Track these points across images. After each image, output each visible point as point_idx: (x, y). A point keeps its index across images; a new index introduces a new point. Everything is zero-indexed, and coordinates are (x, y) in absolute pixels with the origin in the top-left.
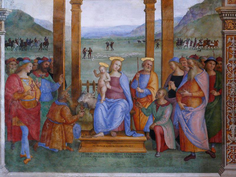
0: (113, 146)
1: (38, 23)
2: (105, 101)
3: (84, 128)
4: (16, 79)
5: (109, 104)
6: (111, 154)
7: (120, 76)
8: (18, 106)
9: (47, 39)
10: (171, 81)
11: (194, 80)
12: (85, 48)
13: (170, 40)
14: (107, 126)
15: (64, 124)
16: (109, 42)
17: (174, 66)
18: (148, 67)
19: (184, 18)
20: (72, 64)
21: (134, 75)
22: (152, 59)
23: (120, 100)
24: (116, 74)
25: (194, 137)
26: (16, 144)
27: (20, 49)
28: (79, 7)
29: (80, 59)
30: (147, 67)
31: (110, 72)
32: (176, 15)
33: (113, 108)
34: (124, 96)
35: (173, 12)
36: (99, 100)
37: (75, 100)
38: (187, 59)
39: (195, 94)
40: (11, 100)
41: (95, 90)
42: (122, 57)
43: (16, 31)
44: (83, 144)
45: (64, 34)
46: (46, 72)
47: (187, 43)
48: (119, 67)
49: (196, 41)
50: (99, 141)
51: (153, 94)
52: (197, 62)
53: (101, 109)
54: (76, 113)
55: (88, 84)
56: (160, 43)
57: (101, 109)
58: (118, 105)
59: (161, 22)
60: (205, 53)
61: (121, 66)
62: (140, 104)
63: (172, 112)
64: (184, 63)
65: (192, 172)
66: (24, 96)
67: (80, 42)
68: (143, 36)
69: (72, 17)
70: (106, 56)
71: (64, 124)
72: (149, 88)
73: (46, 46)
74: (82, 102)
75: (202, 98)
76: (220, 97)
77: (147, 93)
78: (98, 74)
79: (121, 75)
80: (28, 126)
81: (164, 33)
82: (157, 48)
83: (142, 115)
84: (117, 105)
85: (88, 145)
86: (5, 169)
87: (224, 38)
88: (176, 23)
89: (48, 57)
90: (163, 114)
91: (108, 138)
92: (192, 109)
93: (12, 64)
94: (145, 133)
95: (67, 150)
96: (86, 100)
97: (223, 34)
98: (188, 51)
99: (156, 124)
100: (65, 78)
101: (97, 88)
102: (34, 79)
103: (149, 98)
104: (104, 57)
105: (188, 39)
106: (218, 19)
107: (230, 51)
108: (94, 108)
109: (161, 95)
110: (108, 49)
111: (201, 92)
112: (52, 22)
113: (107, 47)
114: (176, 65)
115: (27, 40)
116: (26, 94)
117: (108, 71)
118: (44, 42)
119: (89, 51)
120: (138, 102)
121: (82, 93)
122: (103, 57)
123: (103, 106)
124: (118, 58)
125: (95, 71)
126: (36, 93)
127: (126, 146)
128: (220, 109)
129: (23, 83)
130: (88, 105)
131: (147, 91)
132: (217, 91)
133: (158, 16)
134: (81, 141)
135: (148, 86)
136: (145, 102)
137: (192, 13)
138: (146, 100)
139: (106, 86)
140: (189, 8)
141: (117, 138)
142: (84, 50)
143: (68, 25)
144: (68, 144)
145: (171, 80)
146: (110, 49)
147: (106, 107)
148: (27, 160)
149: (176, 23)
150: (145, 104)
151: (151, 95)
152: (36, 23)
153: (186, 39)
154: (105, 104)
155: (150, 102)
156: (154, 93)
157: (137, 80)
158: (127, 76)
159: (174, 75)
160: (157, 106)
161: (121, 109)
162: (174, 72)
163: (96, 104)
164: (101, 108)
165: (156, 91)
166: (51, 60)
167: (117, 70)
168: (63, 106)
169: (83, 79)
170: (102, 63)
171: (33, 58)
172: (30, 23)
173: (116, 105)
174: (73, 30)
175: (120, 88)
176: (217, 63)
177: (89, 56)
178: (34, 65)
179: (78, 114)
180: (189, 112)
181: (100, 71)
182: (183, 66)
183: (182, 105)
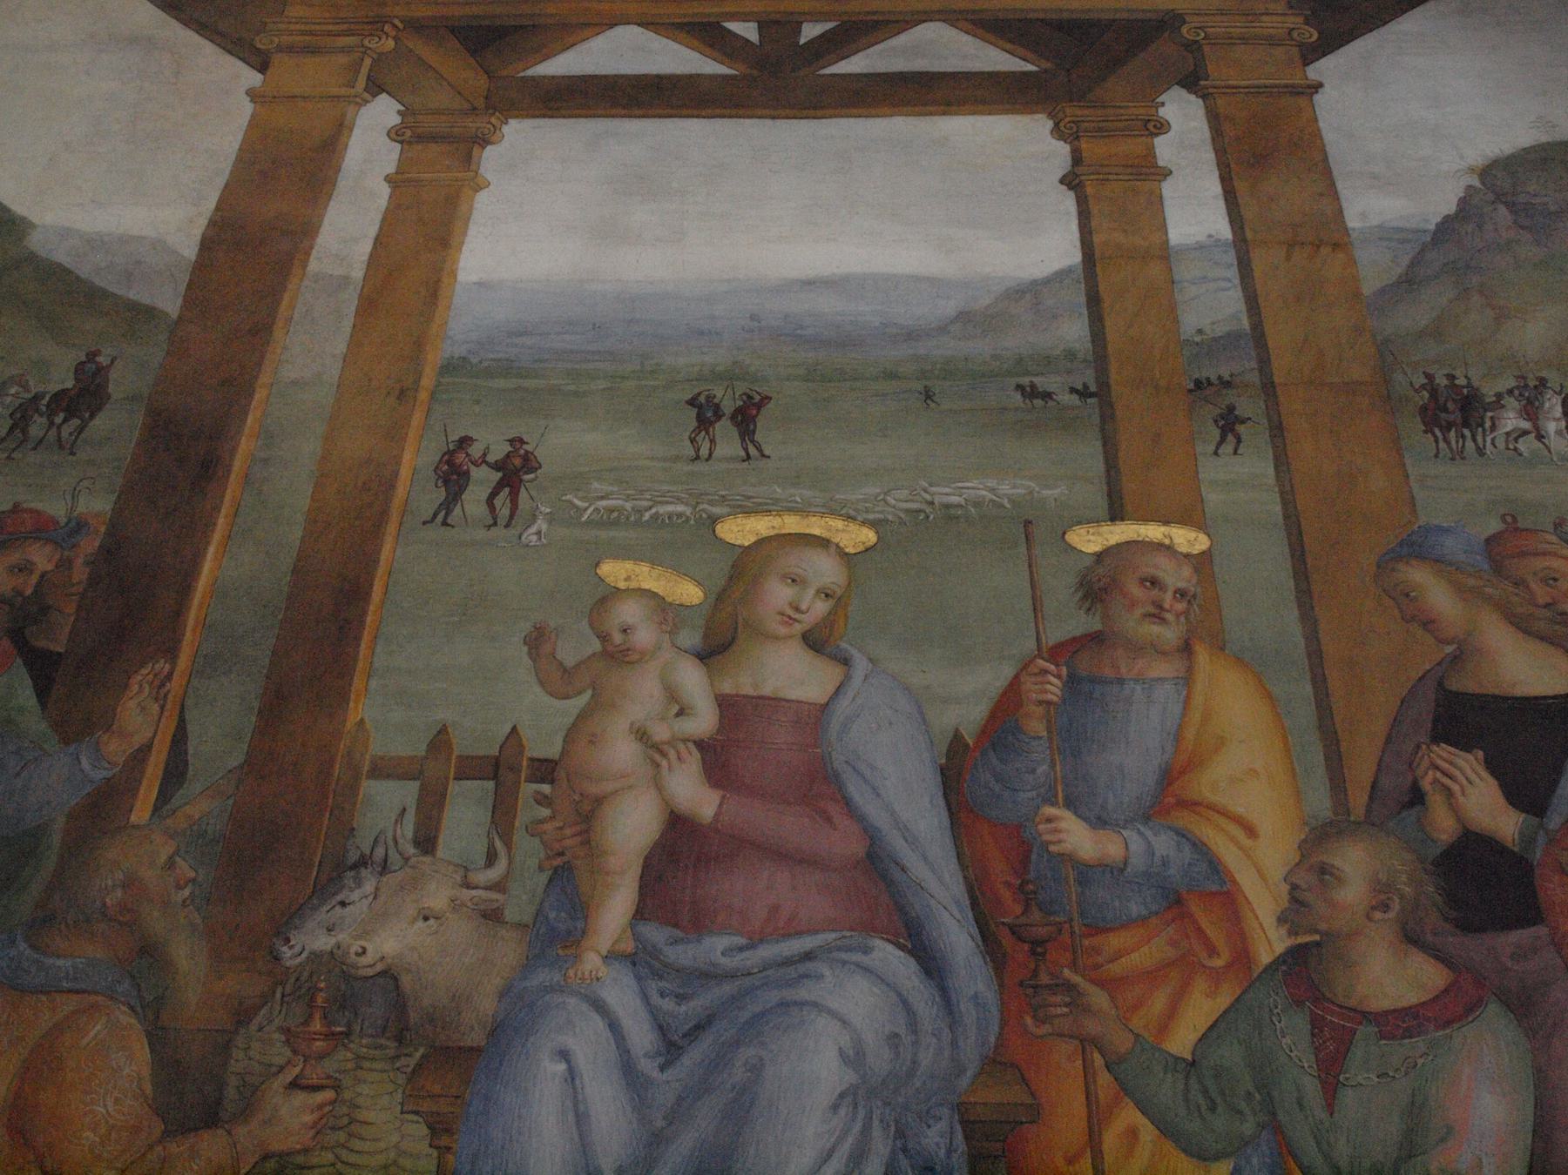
2: (632, 960)
5: (681, 998)
7: (831, 689)
9: (100, 370)
10: (1443, 751)
12: (465, 442)
16: (719, 392)
17: (1439, 597)
18: (1152, 610)
19: (1447, 228)
20: (295, 571)
21: (989, 679)
22: (1187, 539)
23: (828, 949)
28: (468, 161)
29: (391, 528)
30: (1139, 611)
32: (1363, 215)
33: (736, 1043)
35: (1332, 191)
41: (520, 838)
42: (849, 518)
45: (278, 333)
47: (1531, 411)
48: (821, 608)
51: (1247, 881)
53: (564, 1055)
54: (219, 1102)
56: (1249, 406)
57: (564, 1055)
58: (801, 1004)
59: (1231, 257)
61: (839, 592)
62: (1099, 998)
63: (1538, 1104)
67: (423, 396)
68: (1070, 355)
69: (384, 219)
70: (680, 508)
72: (1183, 819)
73: (76, 422)
74: (333, 960)
77: (1172, 871)
78: (578, 666)
79: (847, 678)
81: (1280, 337)
82: (1228, 448)
83: (1132, 1133)
84: (784, 1005)
89: (57, 509)
100: (189, 702)
101: (545, 812)
103: (1199, 930)
104: (656, 517)
105: (1532, 383)
108: (476, 1038)
109: (1353, 892)
110: (704, 452)
113: (698, 430)
117: (691, 638)
118: (69, 384)
119: (497, 466)
120: (1067, 972)
121: (353, 857)
122: (647, 516)
123: (599, 1023)
124: (816, 527)
125: (537, 641)
130: (400, 1004)
131: (1164, 844)
136: (1153, 976)
137: (1506, 204)
138: (1171, 953)
139: (659, 788)
140: (1472, 170)
142: (449, 457)
143: (339, 272)
145: (1436, 739)
146: (727, 442)
147: (641, 1037)
150: (1159, 1002)
151: (1228, 899)
152: (42, 253)
153: (1512, 383)
154: (621, 993)
155: (1216, 977)
157: (1037, 727)
158: (907, 689)
160: (1317, 1024)
161: (841, 1053)
162: (1457, 659)
163: (503, 994)
164: (571, 1043)
166: (79, 526)
167: (798, 629)
168: (69, 1004)
170: (629, 565)
173: (763, 1014)
174: (369, 305)
175: (834, 810)
177: (498, 502)
179: (248, 1107)
181: (604, 638)
182: (1541, 601)
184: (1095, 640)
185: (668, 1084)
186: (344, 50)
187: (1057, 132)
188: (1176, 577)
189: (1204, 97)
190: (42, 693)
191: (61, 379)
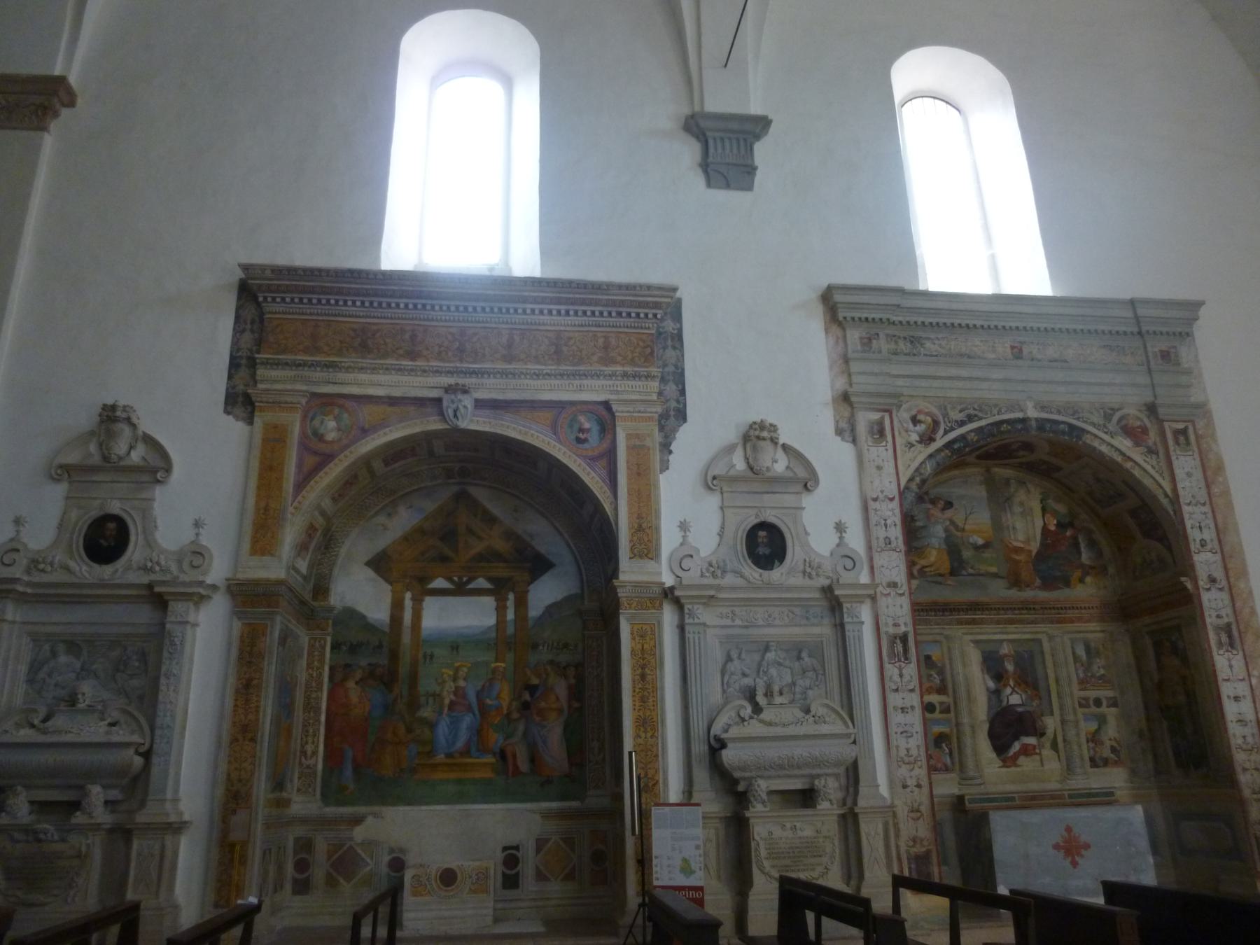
17: (529, 672)
22: (503, 665)
24: (462, 683)
31: (455, 679)
34: (469, 709)
36: (440, 713)
47: (543, 646)
49: (553, 644)
60: (563, 658)
75: (560, 711)
88: (531, 623)
94: (494, 754)
99: (507, 743)
125: (436, 680)
133: (510, 615)
135: (498, 697)
146: (455, 652)
147: (449, 723)
149: (531, 623)
156: (505, 704)
171: (364, 662)
183: (537, 719)
187: (495, 600)
188: (501, 670)
189: (514, 593)
191: (377, 643)
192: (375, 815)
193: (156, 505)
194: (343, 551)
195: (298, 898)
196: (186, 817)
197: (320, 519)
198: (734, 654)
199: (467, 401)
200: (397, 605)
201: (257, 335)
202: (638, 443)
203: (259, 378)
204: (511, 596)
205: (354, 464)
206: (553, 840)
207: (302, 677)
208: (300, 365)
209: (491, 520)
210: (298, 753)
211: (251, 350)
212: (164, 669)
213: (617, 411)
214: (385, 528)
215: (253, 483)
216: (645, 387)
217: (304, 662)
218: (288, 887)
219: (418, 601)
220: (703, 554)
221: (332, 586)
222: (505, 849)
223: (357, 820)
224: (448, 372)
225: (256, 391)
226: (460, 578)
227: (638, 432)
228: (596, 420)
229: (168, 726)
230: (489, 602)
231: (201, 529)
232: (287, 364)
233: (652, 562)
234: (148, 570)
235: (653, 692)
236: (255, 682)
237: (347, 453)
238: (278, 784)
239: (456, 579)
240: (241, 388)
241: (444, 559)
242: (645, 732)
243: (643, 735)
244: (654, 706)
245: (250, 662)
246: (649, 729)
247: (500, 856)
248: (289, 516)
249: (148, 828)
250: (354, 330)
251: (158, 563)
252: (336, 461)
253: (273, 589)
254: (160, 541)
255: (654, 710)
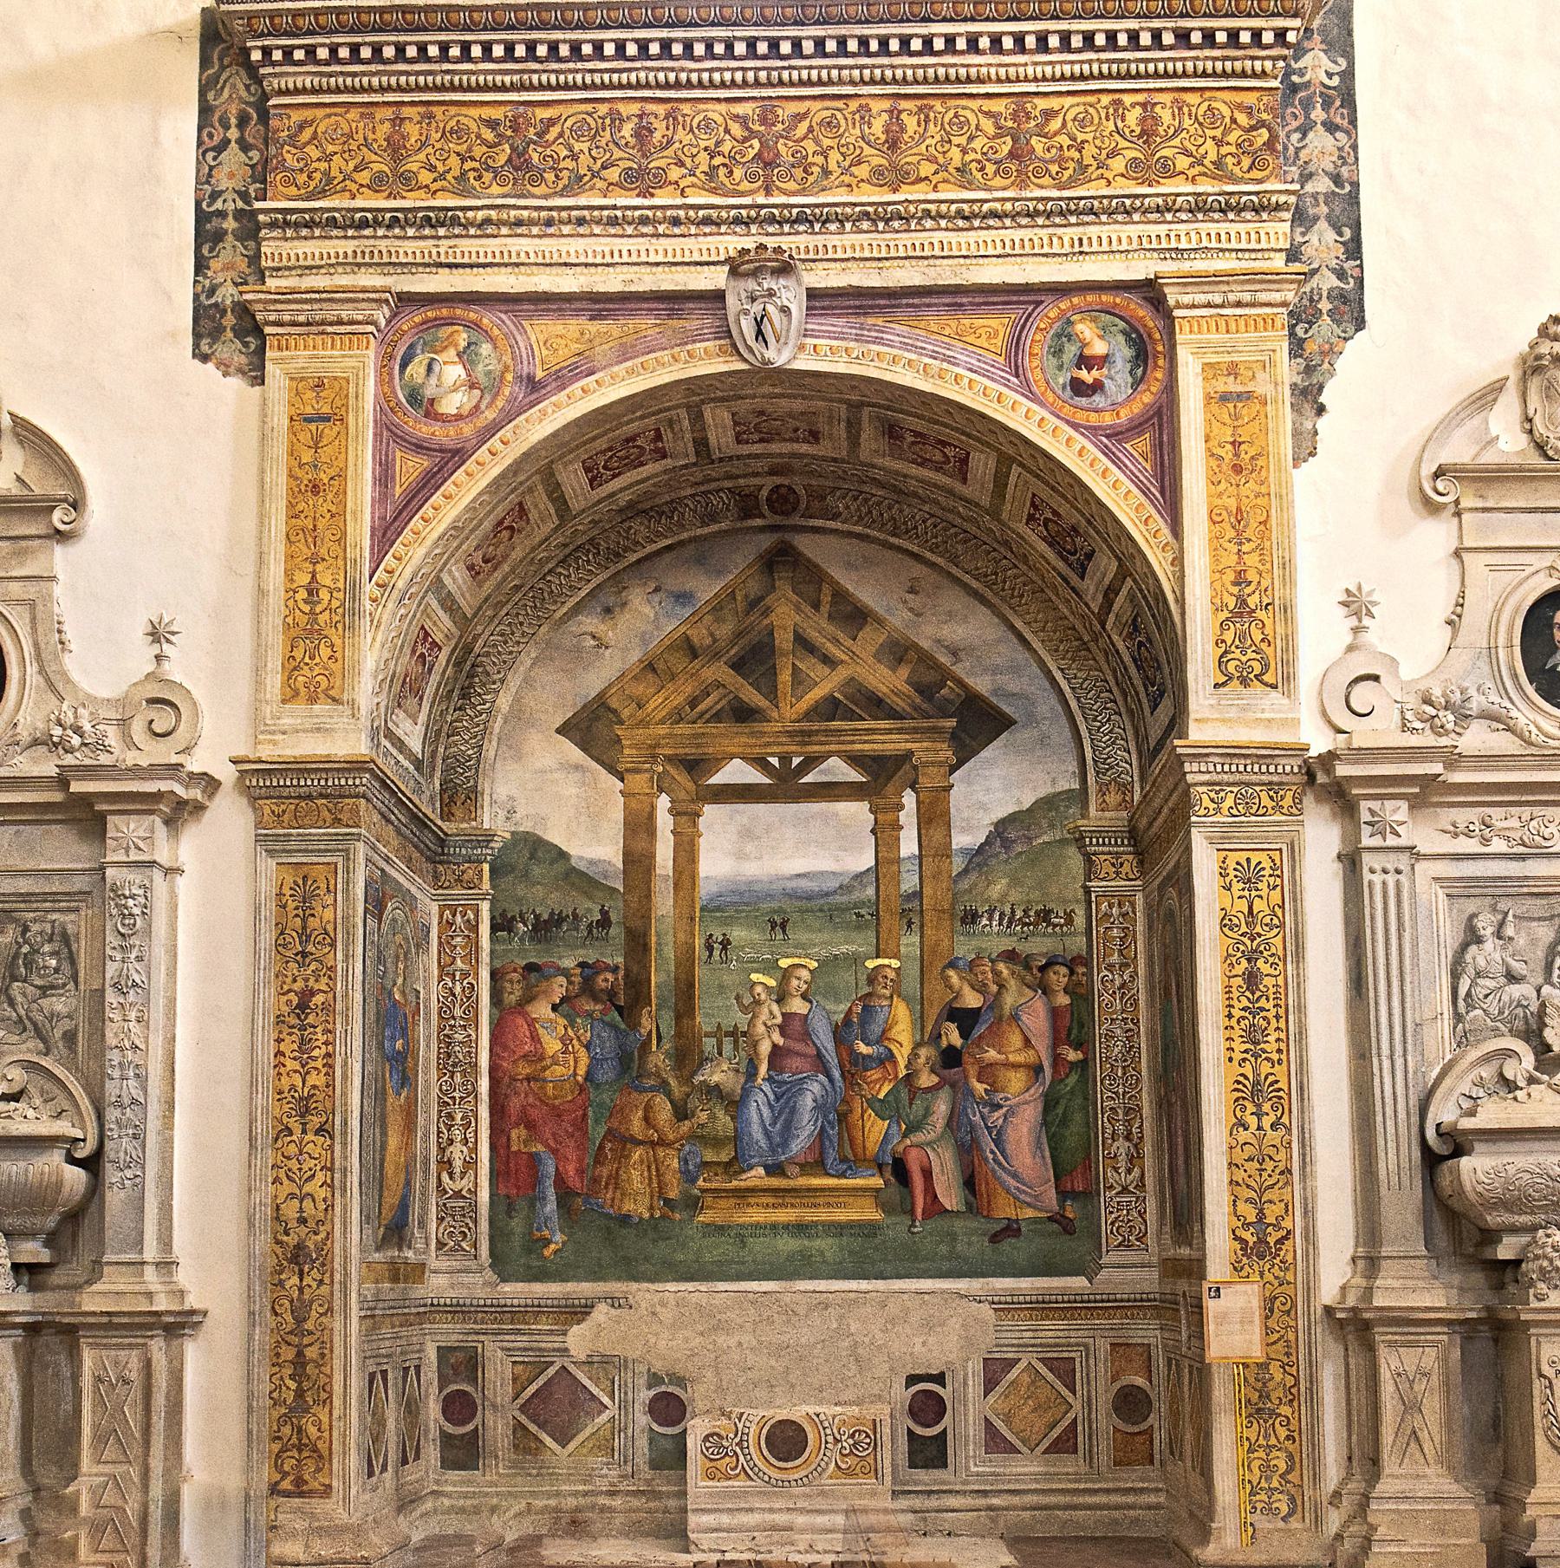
0: (793, 1206)
1: (582, 866)
3: (709, 1156)
4: (520, 1021)
6: (786, 1226)
8: (526, 1095)
11: (1015, 1018)
13: (943, 911)
14: (773, 1150)
15: (653, 1145)
21: (844, 1007)
22: (895, 963)
24: (798, 1006)
25: (1015, 1176)
26: (521, 1204)
27: (532, 939)
28: (695, 824)
37: (688, 1080)
38: (992, 961)
39: (1012, 1058)
40: (506, 1079)
43: (521, 891)
44: (709, 1200)
46: (603, 1003)
47: (990, 919)
49: (1013, 912)
50: (752, 1191)
51: (899, 1058)
52: (1017, 968)
55: (719, 1033)
56: (916, 920)
60: (1039, 946)
64: (984, 973)
65: (1014, 1276)
66: (545, 1069)
71: (653, 1144)
72: (886, 1043)
75: (1037, 1070)
76: (1084, 1065)
80: (555, 1152)
81: (927, 891)
85: (723, 1203)
86: (489, 1275)
87: (1089, 903)
88: (958, 864)
89: (609, 961)
90: (928, 1112)
91: (775, 1182)
92: (1007, 1099)
93: (511, 982)
94: (880, 1167)
95: (663, 1217)
96: (716, 1078)
97: (1087, 891)
98: (993, 938)
99: (908, 1142)
102: (572, 1024)
106: (1072, 851)
107: (1107, 939)
109: (922, 1060)
111: (1031, 1052)
112: (621, 866)
114: (961, 978)
115: (552, 914)
116: (549, 1062)
117: (774, 997)
125: (738, 998)
126: (576, 1062)
127: (829, 1205)
128: (1086, 1099)
129: (541, 1031)
132: (1076, 1050)
133: (909, 845)
134: (704, 1191)
135: (883, 1037)
141: (803, 1181)
144: (667, 1201)
147: (772, 1097)
148: (553, 1246)
151: (895, 1063)
154: (766, 1087)
159: (956, 1005)
165: (906, 1050)
166: (615, 969)
169: (703, 1022)
172: (559, 867)
174: (676, 885)
176: (1072, 972)
178: (570, 982)
180: (1000, 1107)
183: (980, 1088)
184: (869, 995)
185: (777, 1106)
186: (646, 771)
188: (891, 975)
190: (621, 1015)
192: (614, 1301)
193: (58, 590)
194: (504, 702)
195: (454, 1475)
196: (192, 1302)
197: (446, 620)
198: (1485, 925)
199: (791, 294)
200: (639, 827)
201: (255, 155)
202: (1233, 387)
203: (270, 264)
204: (909, 799)
205: (515, 468)
206: (1022, 1365)
207: (431, 992)
208: (364, 224)
209: (854, 616)
210: (433, 1167)
211: (244, 196)
212: (111, 969)
213: (1178, 306)
214: (602, 644)
215: (278, 522)
216: (1253, 236)
217: (430, 961)
218: (432, 1453)
219: (686, 815)
220: (1406, 673)
221: (485, 785)
222: (912, 1380)
223: (578, 1312)
224: (737, 221)
225: (262, 296)
226: (785, 759)
227: (1236, 358)
228: (1123, 332)
229: (134, 1102)
230: (858, 812)
231: (165, 646)
232: (332, 223)
233: (1274, 694)
234: (55, 745)
235: (1277, 1017)
236: (319, 999)
237: (494, 442)
238: (395, 1231)
239: (774, 761)
240: (227, 294)
241: (743, 714)
242: (1259, 1115)
243: (1252, 1121)
244: (1279, 1051)
245: (304, 954)
246: (1266, 1107)
247: (902, 1395)
248: (368, 605)
249: (112, 1326)
250: (492, 124)
251: (78, 730)
252: (470, 465)
253: (343, 782)
254: (75, 676)
255: (1280, 1062)
